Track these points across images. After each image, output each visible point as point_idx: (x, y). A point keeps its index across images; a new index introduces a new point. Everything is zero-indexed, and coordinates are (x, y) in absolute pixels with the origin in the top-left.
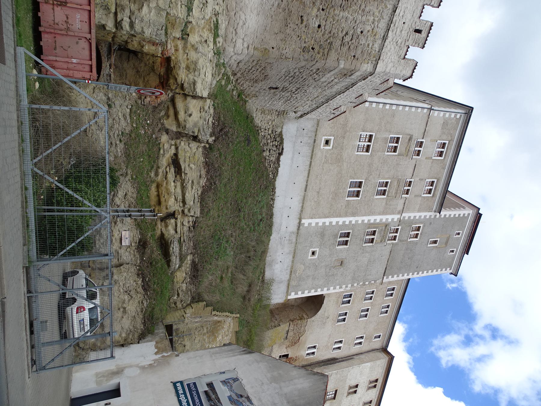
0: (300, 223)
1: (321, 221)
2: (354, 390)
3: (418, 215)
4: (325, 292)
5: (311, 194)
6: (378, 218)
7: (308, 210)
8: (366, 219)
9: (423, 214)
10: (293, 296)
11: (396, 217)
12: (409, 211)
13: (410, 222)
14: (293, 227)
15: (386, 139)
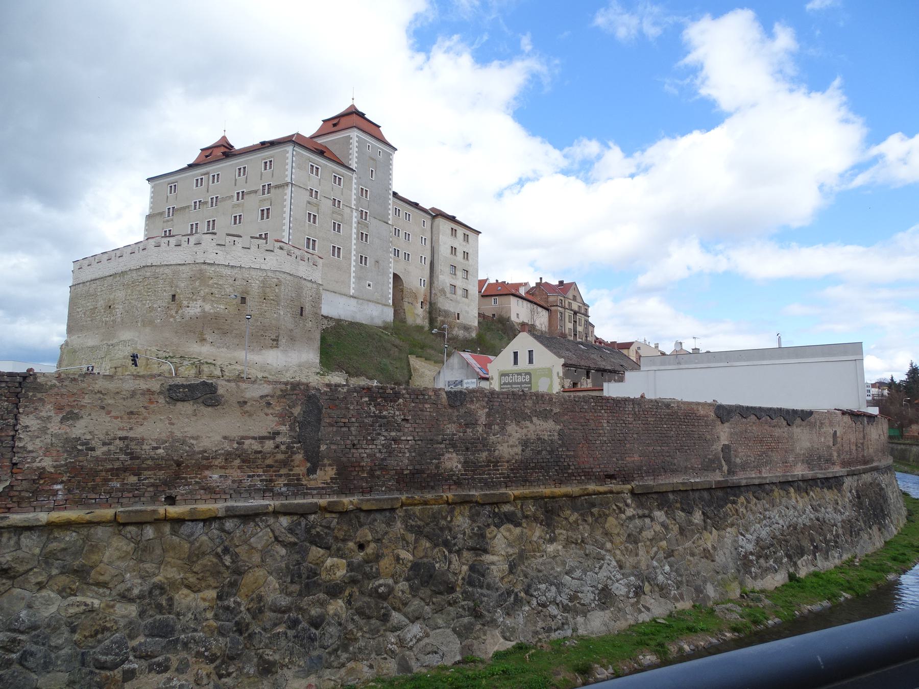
1: (353, 280)
2: (454, 250)
4: (392, 271)
6: (354, 231)
8: (354, 241)
9: (354, 186)
10: (391, 302)
11: (355, 214)
12: (350, 200)
13: (358, 200)
14: (353, 302)
15: (310, 225)
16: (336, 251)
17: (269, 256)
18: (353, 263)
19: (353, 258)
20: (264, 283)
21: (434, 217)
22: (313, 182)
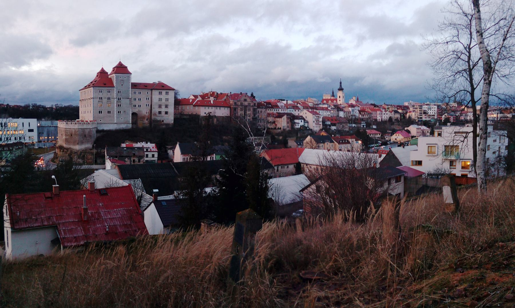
13: (117, 95)
16: (109, 112)
20: (75, 132)
21: (152, 90)
22: (101, 95)
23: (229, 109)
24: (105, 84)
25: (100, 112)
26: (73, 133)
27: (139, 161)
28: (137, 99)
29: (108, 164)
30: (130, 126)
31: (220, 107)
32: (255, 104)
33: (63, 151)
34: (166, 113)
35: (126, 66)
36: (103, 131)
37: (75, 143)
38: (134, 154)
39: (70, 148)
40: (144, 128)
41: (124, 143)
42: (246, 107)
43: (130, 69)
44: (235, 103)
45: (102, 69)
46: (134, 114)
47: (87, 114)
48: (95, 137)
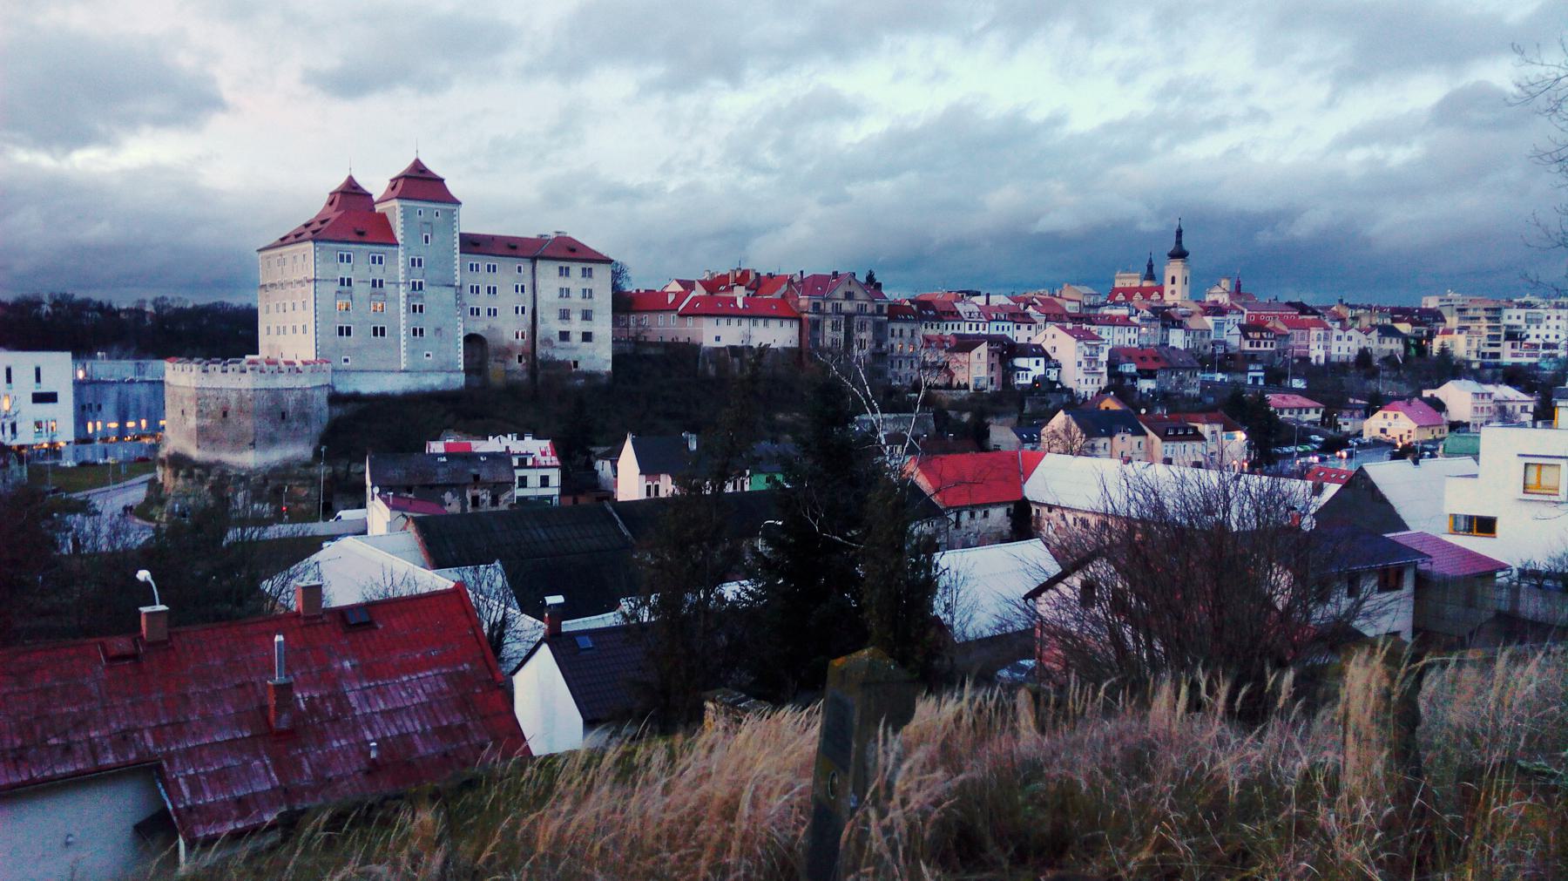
0: (405, 371)
3: (401, 265)
5: (383, 366)
6: (403, 305)
7: (395, 367)
8: (402, 316)
10: (461, 367)
13: (408, 272)
16: (379, 332)
17: (243, 377)
18: (403, 338)
19: (403, 333)
20: (241, 399)
21: (534, 260)
22: (345, 270)
23: (796, 325)
24: (361, 234)
25: (344, 331)
26: (233, 405)
27: (495, 501)
28: (484, 291)
29: (378, 513)
30: (459, 380)
31: (767, 318)
32: (880, 308)
33: (190, 475)
34: (587, 337)
35: (439, 172)
36: (356, 397)
37: (238, 444)
38: (476, 477)
39: (218, 463)
40: (511, 389)
41: (436, 438)
42: (849, 317)
43: (453, 187)
44: (816, 306)
45: (351, 179)
46: (473, 342)
47: (291, 335)
48: (326, 421)
